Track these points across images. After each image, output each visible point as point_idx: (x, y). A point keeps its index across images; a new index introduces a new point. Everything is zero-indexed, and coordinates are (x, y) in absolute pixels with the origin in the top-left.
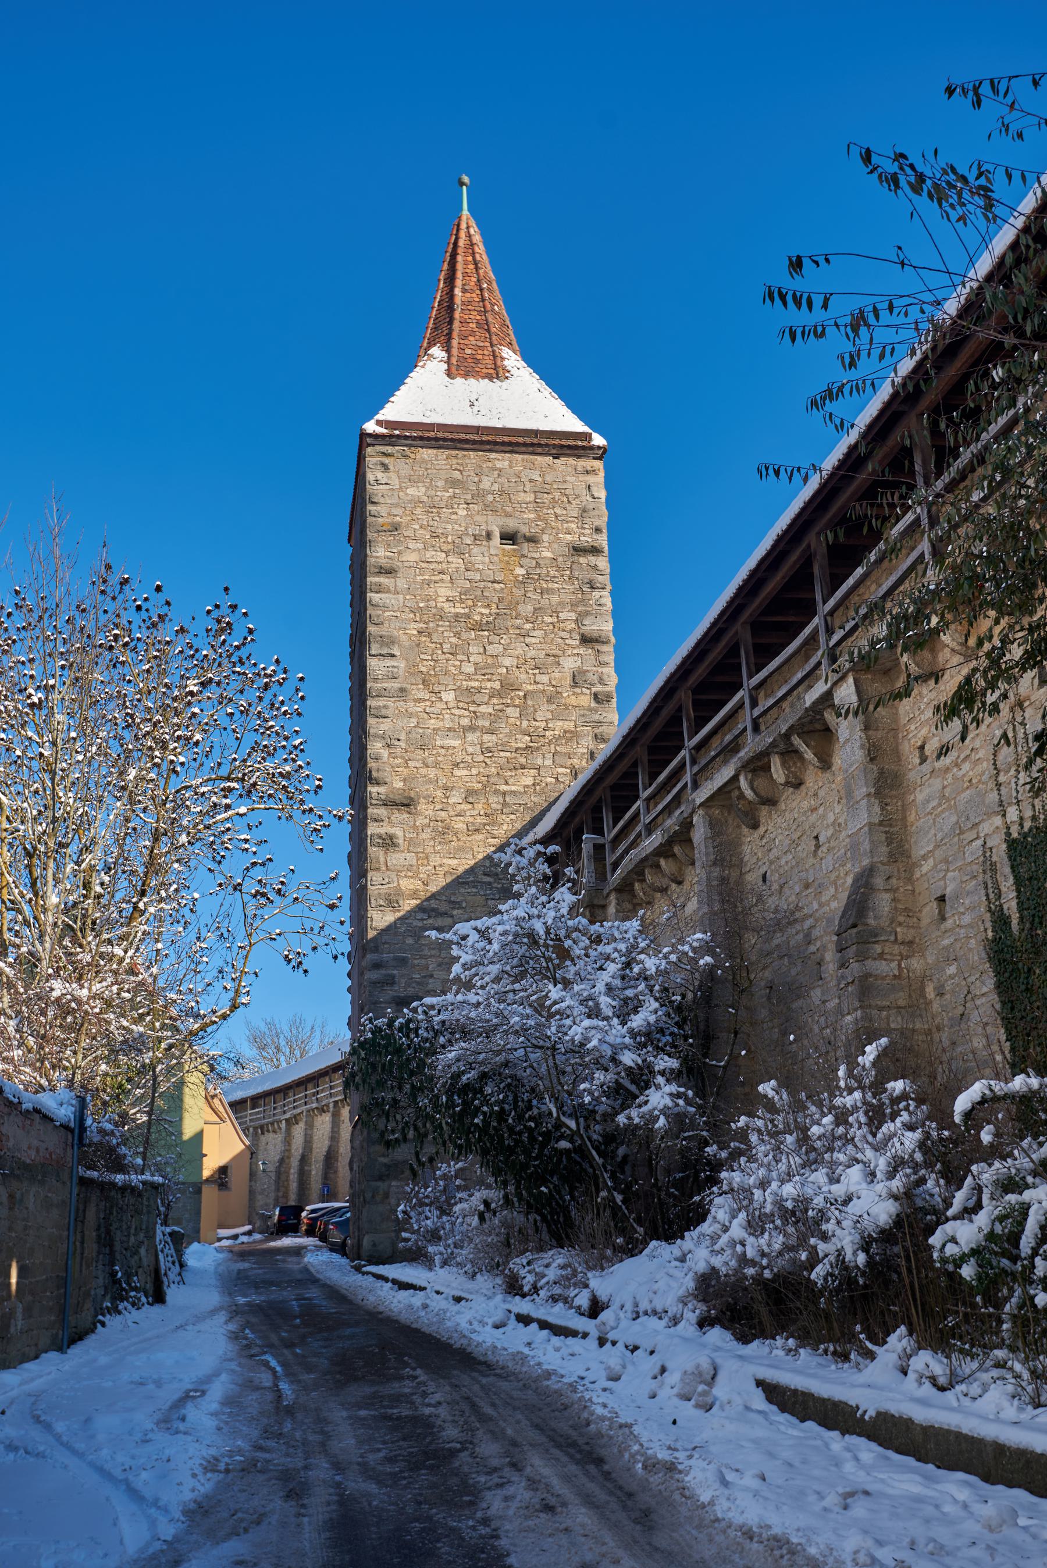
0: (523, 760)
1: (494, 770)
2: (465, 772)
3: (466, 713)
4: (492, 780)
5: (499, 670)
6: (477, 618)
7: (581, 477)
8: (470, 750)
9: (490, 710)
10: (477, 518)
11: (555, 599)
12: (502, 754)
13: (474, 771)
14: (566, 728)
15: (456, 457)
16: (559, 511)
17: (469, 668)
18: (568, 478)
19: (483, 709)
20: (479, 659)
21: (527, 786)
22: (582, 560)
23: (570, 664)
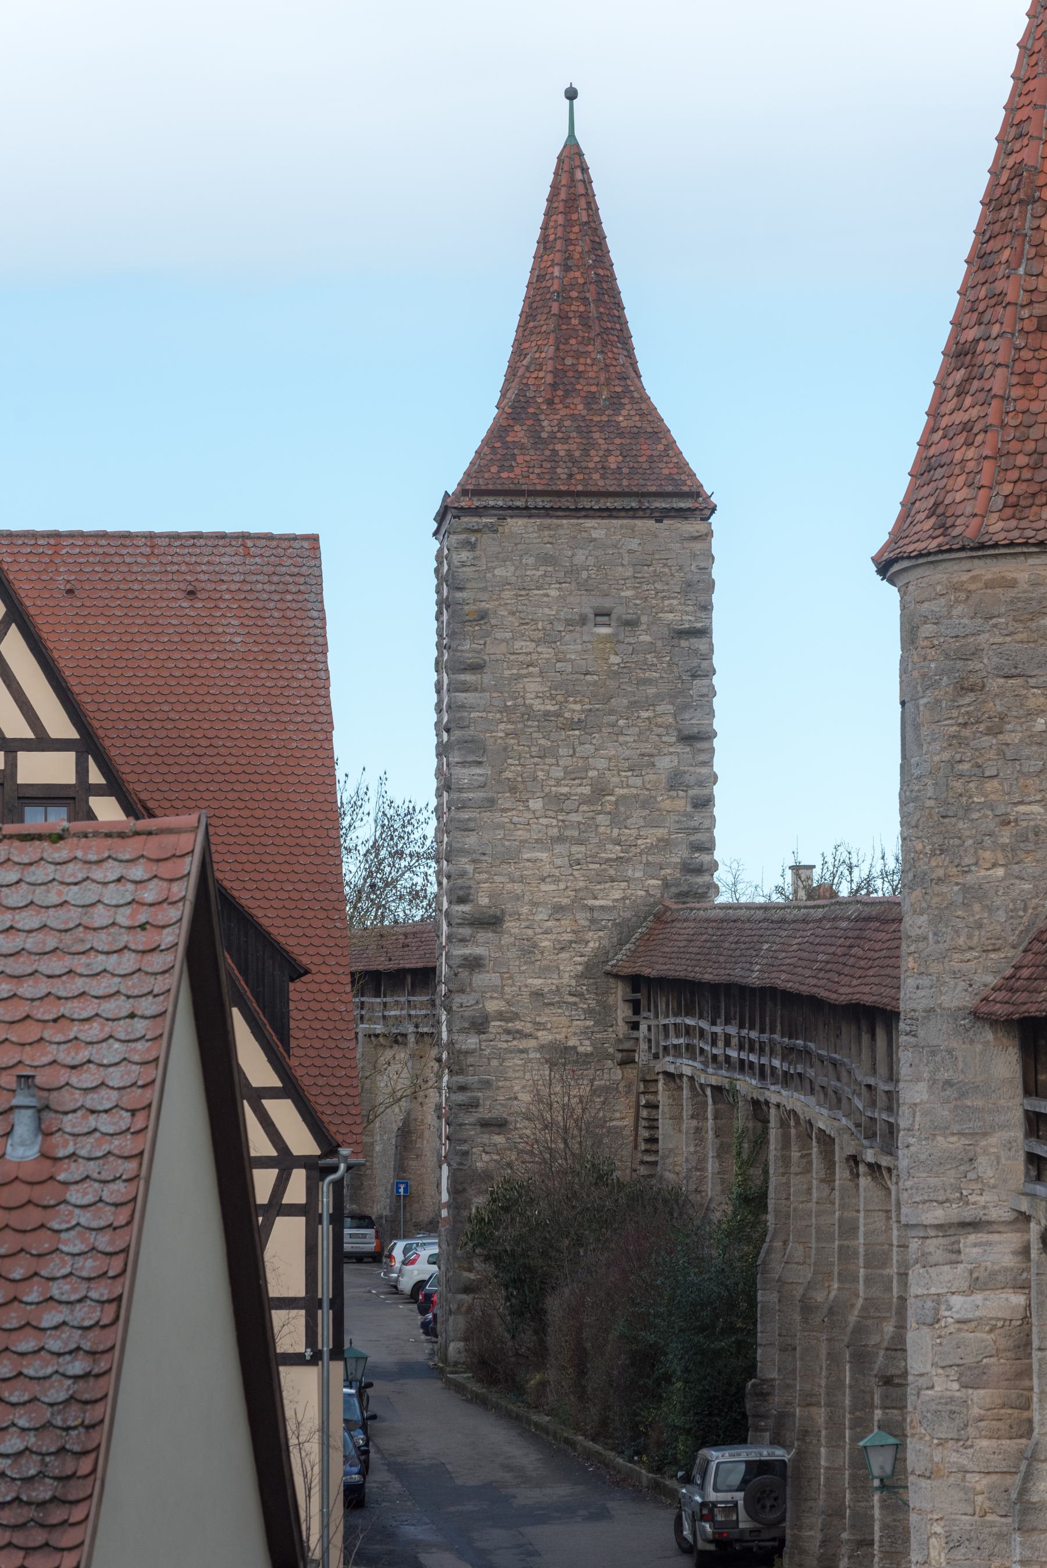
0: (612, 872)
1: (581, 884)
2: (553, 887)
3: (555, 822)
4: (581, 894)
8: (559, 862)
9: (580, 819)
11: (652, 691)
12: (591, 866)
13: (562, 886)
15: (549, 528)
17: (558, 773)
19: (574, 817)
21: (617, 900)
22: (684, 643)
23: (665, 763)
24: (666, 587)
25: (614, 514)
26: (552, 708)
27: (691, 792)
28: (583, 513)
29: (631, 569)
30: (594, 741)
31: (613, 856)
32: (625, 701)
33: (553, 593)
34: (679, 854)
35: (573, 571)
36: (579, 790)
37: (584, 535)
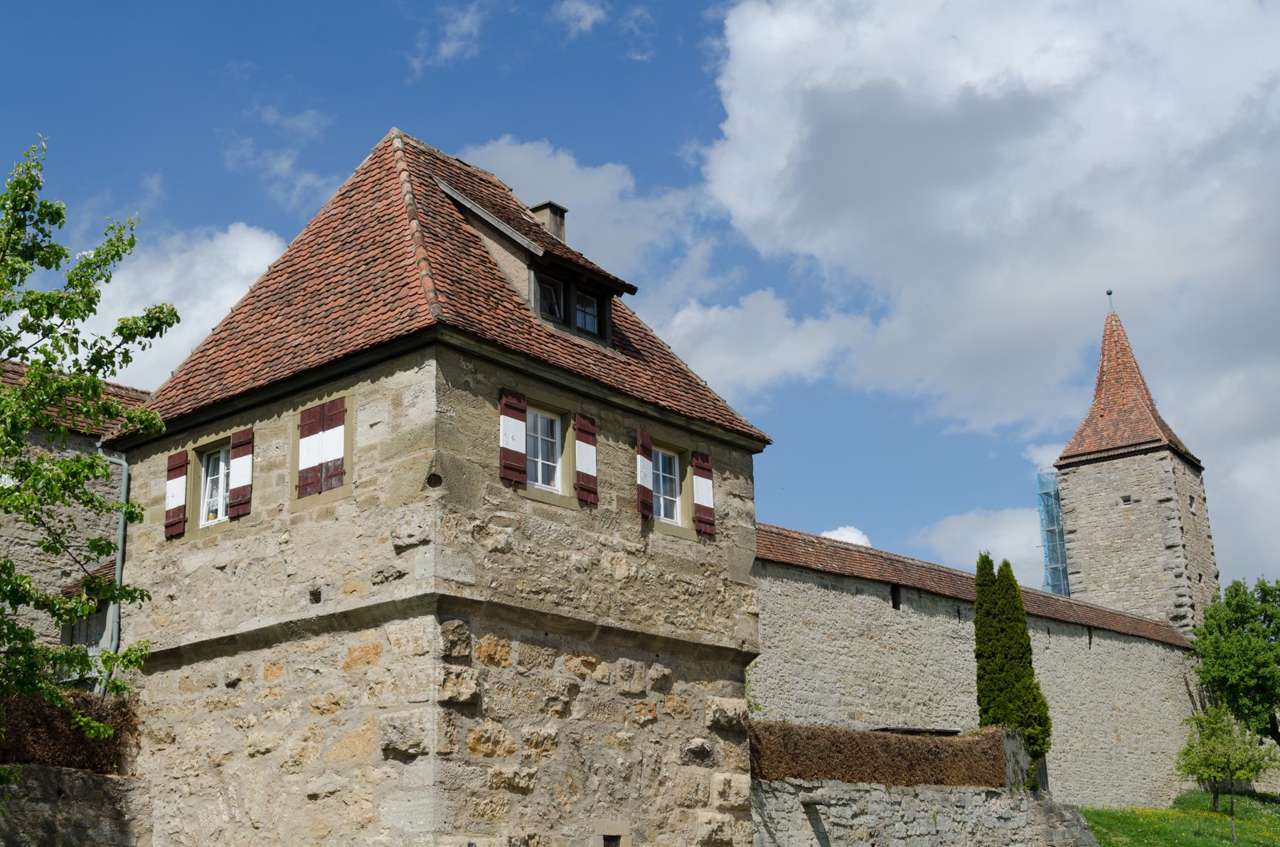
11: (1151, 529)
17: (1113, 571)
22: (1163, 505)
23: (1161, 560)
35: (1111, 482)
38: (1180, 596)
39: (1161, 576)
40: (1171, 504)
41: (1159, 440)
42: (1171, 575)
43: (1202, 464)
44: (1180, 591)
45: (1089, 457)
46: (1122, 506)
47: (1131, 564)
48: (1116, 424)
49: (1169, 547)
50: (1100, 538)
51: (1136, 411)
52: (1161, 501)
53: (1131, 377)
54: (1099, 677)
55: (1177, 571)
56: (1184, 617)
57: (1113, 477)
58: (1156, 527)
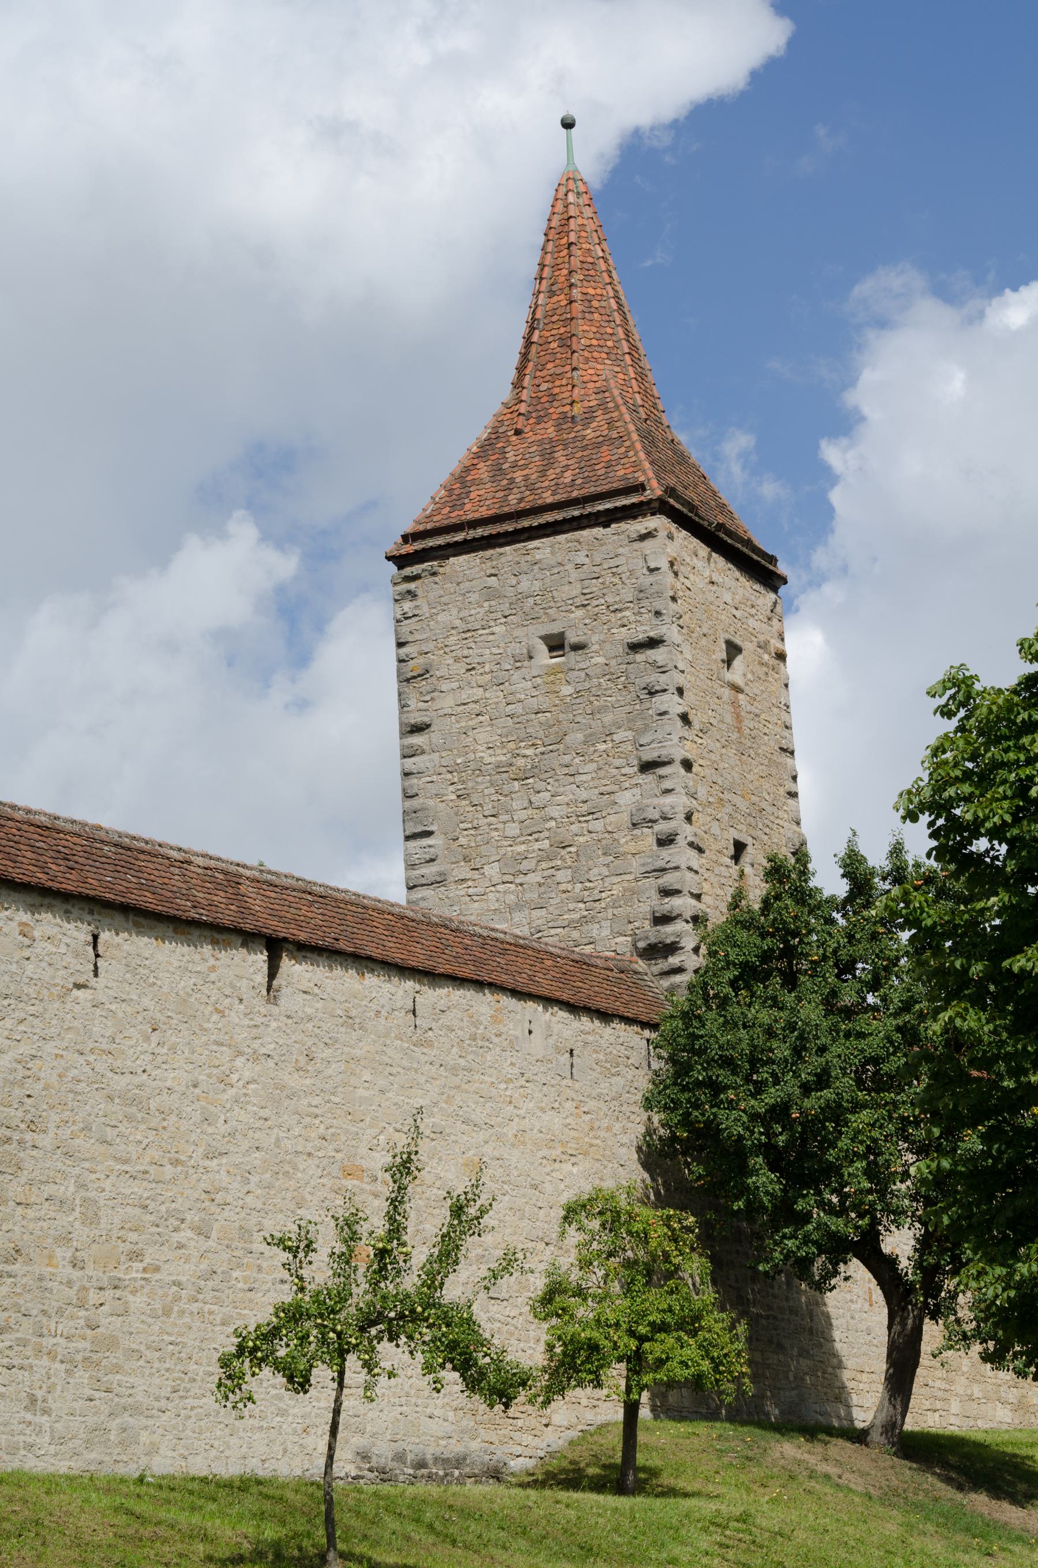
0: (575, 934)
5: (547, 826)
6: (520, 762)
7: (637, 545)
10: (517, 632)
11: (608, 718)
12: (553, 932)
14: (625, 884)
16: (610, 599)
17: (513, 829)
18: (621, 550)
19: (533, 878)
20: (523, 815)
22: (640, 657)
23: (626, 799)
24: (617, 599)
25: (558, 528)
26: (504, 758)
27: (657, 828)
28: (526, 535)
29: (579, 586)
30: (549, 787)
31: (576, 916)
32: (580, 736)
33: (496, 629)
34: (651, 902)
36: (537, 846)
37: (528, 558)
38: (667, 892)
39: (625, 841)
40: (657, 655)
41: (640, 488)
42: (648, 839)
43: (782, 568)
44: (669, 880)
45: (472, 534)
46: (543, 657)
47: (554, 811)
48: (548, 457)
49: (647, 767)
50: (485, 745)
51: (601, 418)
52: (635, 647)
53: (600, 336)
54: (294, 1081)
55: (663, 827)
56: (672, 948)
57: (525, 585)
58: (620, 714)
